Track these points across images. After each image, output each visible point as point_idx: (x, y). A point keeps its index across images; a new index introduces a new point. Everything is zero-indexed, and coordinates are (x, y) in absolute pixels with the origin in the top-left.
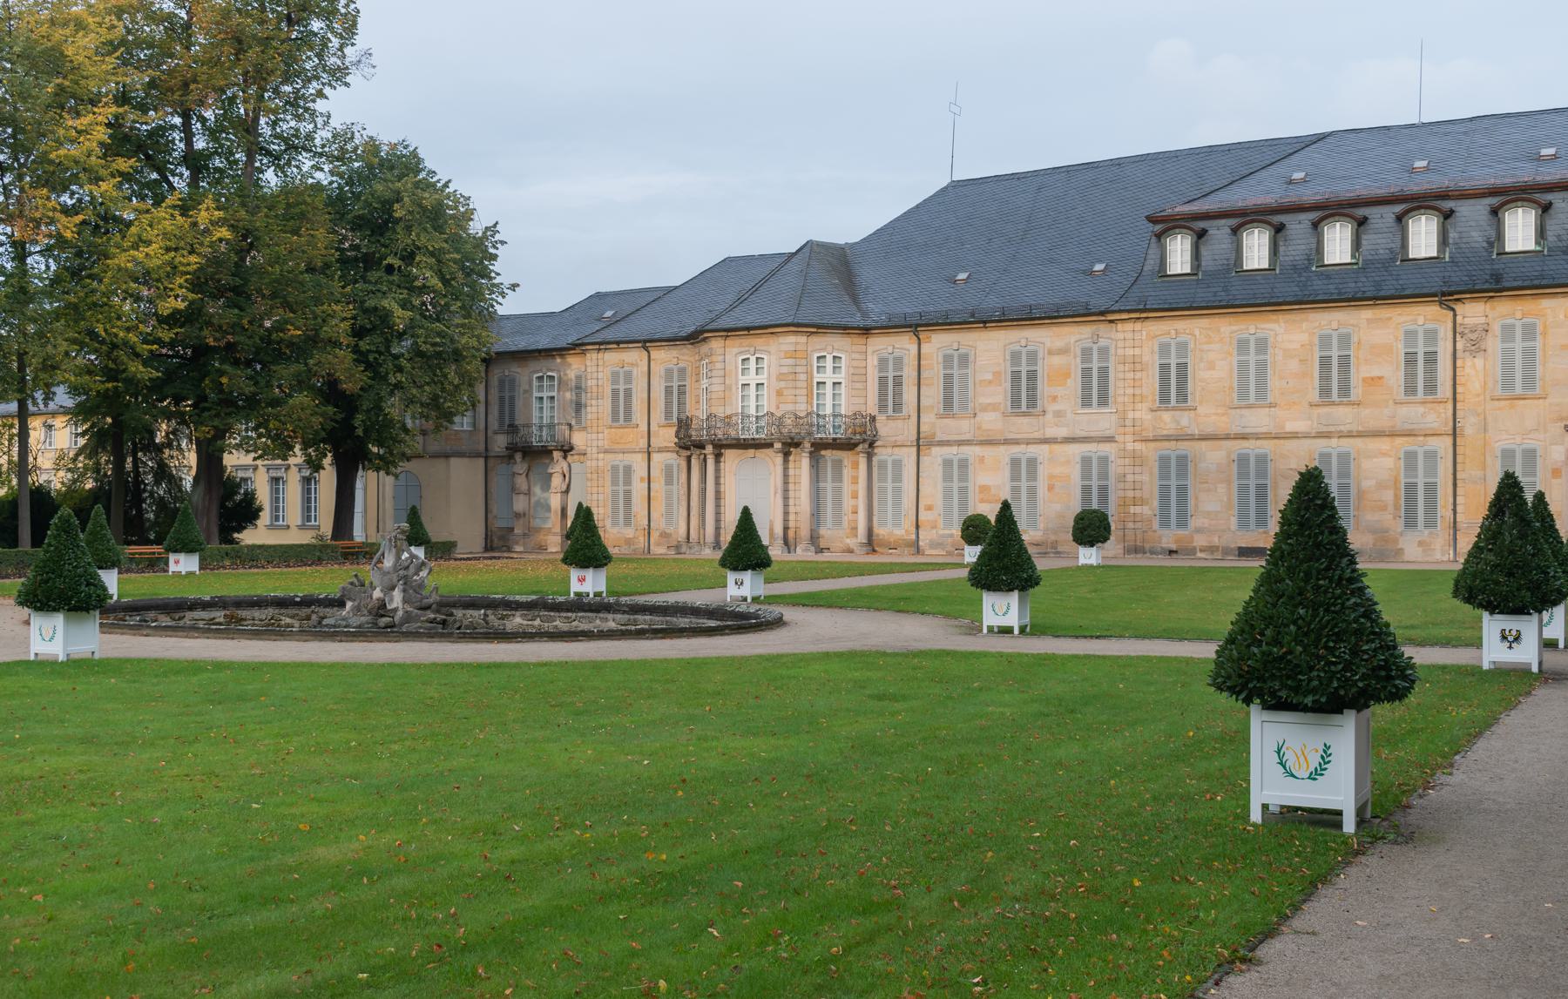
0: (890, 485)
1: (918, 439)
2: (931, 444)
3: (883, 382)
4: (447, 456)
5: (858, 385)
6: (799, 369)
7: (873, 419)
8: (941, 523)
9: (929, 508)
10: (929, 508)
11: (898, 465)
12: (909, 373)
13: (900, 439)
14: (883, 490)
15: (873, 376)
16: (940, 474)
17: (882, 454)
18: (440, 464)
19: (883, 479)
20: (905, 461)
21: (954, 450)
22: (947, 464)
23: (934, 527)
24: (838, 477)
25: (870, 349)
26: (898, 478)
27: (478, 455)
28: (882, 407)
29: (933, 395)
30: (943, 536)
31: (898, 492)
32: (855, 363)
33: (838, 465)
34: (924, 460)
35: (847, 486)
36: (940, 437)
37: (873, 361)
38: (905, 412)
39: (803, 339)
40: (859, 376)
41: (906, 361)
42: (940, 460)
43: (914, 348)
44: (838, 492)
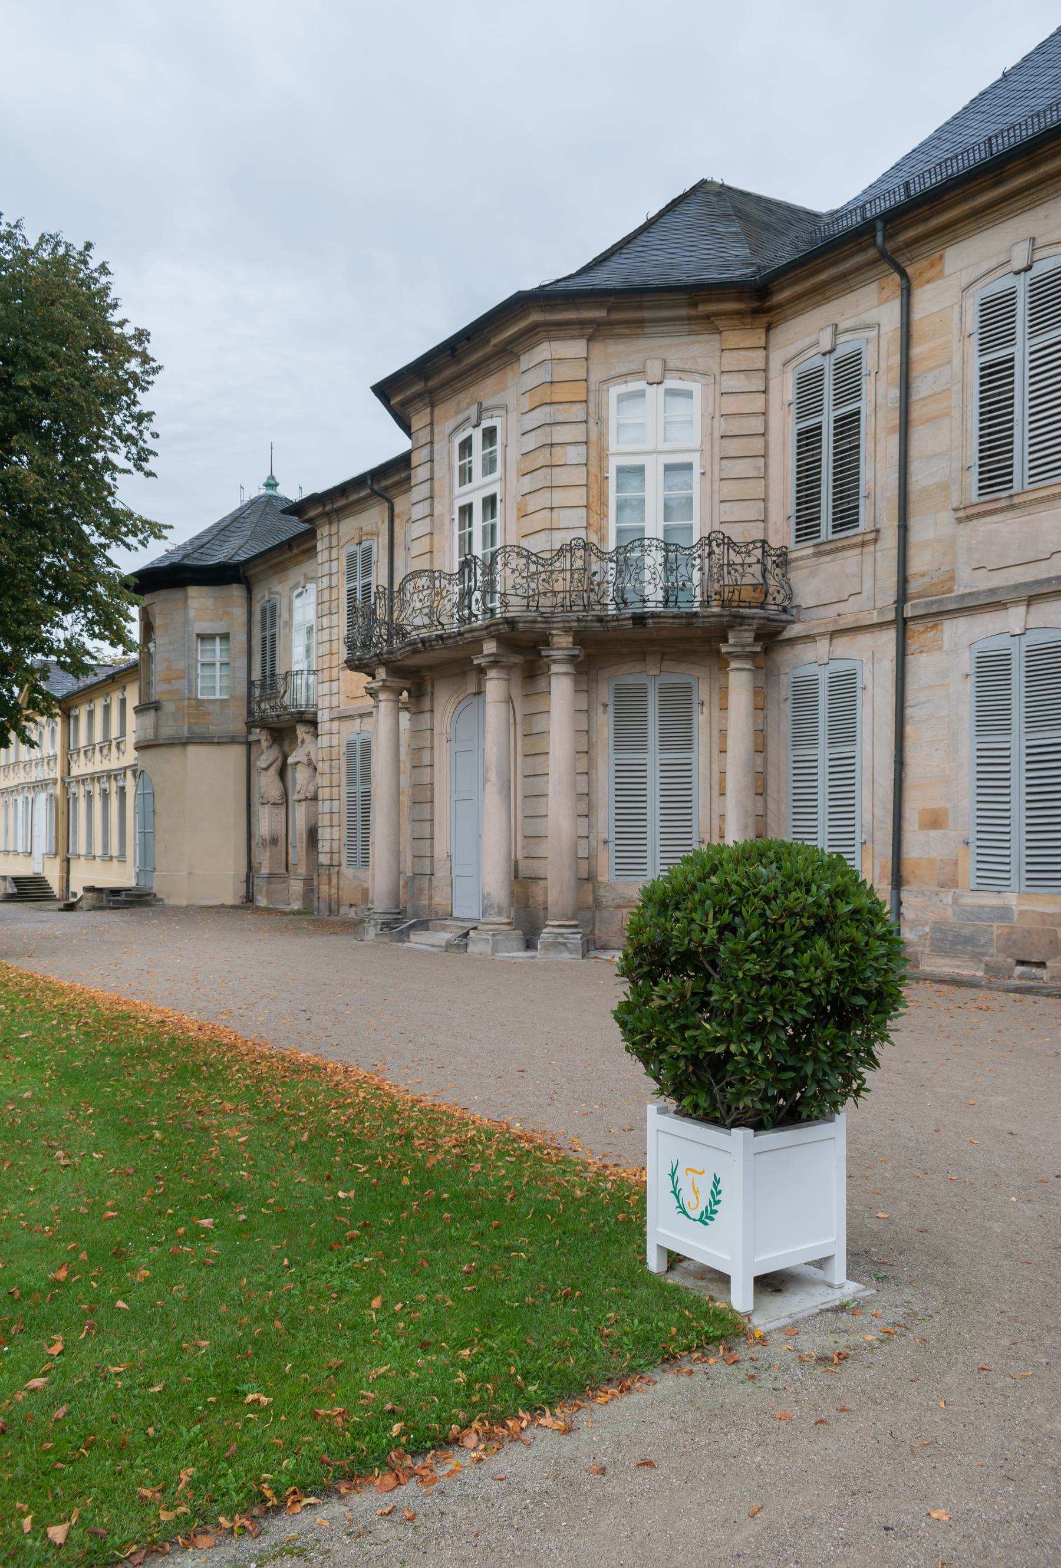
0: (823, 753)
1: (903, 597)
2: (937, 616)
3: (808, 439)
4: (184, 743)
5: (741, 468)
6: (561, 434)
7: (783, 560)
8: (968, 866)
9: (935, 821)
10: (935, 821)
11: (845, 686)
12: (877, 398)
13: (852, 612)
14: (804, 769)
15: (784, 430)
16: (967, 710)
17: (810, 661)
18: (173, 755)
19: (803, 735)
20: (865, 677)
21: (1015, 618)
22: (991, 668)
23: (949, 882)
24: (678, 735)
25: (777, 357)
26: (844, 730)
27: (232, 741)
28: (806, 525)
29: (948, 445)
30: (977, 913)
31: (844, 769)
32: (731, 405)
33: (679, 708)
34: (917, 663)
35: (701, 756)
36: (970, 582)
37: (785, 389)
38: (865, 523)
39: (575, 348)
40: (734, 440)
41: (868, 363)
42: (967, 662)
43: (889, 315)
44: (678, 777)
